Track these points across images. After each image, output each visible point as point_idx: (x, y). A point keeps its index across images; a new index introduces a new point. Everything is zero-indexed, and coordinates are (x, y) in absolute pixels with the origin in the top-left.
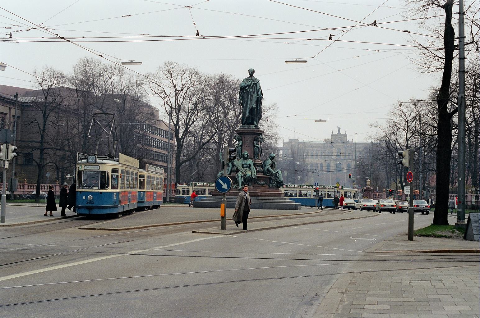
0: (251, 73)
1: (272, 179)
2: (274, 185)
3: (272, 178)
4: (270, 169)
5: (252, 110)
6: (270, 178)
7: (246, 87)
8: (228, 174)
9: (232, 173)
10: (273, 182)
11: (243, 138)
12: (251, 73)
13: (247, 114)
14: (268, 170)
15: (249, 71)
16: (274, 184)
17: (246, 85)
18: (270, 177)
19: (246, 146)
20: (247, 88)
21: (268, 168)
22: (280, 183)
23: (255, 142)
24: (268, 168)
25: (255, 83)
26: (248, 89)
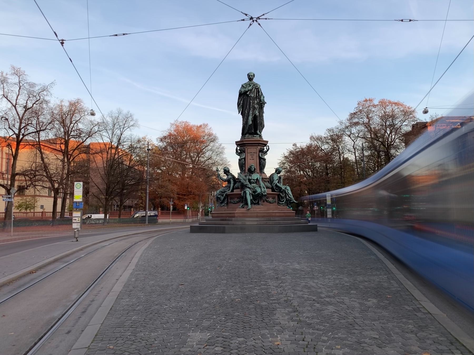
0: (251, 77)
1: (282, 197)
3: (281, 194)
4: (278, 184)
5: (255, 118)
6: (279, 195)
7: (247, 92)
8: (230, 191)
9: (235, 190)
11: (246, 149)
12: (251, 77)
13: (250, 122)
14: (276, 185)
15: (248, 75)
16: (283, 201)
18: (279, 194)
20: (248, 93)
22: (291, 200)
23: (260, 154)
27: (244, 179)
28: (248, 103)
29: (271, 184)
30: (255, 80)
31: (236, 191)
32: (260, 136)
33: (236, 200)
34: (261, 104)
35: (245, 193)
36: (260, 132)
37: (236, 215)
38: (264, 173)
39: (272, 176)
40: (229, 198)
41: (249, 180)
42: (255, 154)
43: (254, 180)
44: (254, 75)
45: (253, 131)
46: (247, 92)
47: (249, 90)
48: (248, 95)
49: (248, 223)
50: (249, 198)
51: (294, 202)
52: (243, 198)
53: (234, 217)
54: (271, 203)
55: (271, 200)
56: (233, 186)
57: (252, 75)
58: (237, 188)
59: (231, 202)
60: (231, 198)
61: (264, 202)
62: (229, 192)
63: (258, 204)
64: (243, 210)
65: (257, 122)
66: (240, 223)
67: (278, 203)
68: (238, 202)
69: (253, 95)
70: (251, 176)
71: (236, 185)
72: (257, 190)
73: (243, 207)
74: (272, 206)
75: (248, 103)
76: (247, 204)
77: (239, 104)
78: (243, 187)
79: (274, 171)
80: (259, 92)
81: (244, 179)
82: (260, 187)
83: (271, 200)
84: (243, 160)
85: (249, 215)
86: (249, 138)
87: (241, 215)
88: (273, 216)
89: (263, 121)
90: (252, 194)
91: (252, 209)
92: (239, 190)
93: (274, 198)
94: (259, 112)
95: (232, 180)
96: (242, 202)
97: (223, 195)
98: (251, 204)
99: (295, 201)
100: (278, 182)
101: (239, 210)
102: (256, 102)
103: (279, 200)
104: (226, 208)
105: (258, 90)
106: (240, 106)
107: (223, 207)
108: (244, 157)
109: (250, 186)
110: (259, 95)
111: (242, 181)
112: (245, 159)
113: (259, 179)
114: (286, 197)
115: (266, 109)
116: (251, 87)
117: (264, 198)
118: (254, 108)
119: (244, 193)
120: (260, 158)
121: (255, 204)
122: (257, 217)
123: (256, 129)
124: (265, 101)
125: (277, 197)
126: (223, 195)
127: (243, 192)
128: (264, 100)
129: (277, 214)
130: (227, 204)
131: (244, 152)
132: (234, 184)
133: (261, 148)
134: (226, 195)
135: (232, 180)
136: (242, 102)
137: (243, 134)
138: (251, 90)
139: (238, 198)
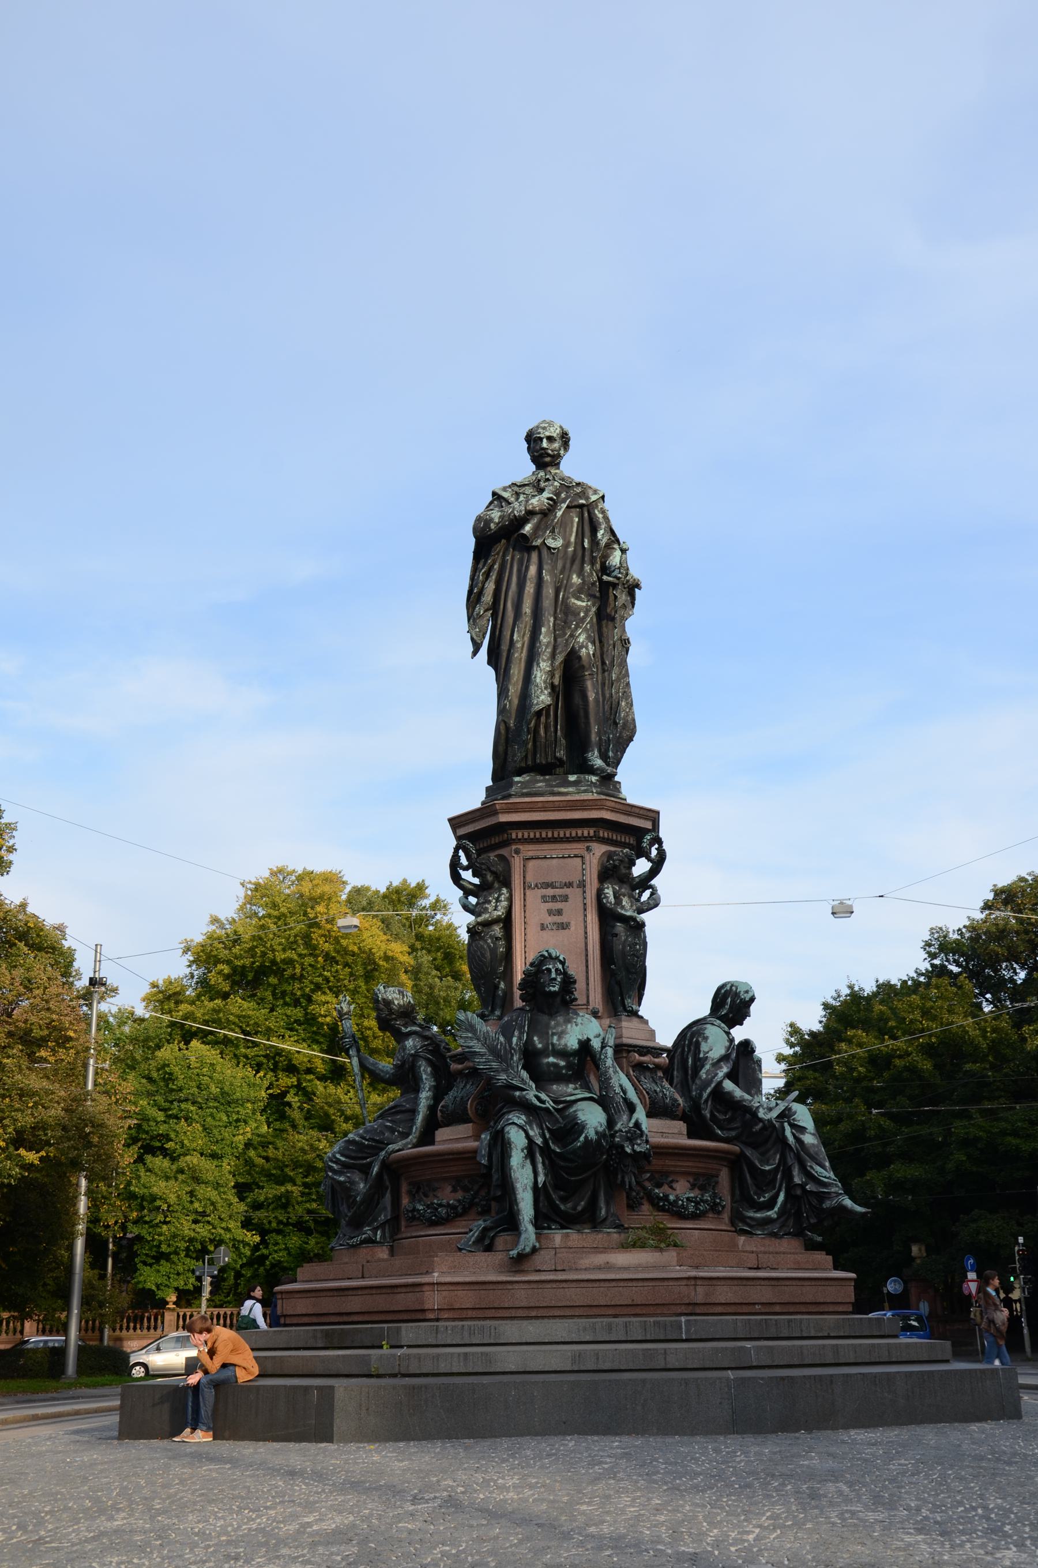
1: (753, 1170)
2: (772, 1214)
4: (729, 1085)
5: (571, 671)
7: (522, 521)
8: (412, 1138)
10: (761, 1192)
11: (517, 863)
12: (544, 451)
13: (542, 698)
14: (718, 1093)
16: (770, 1204)
17: (518, 508)
19: (543, 927)
20: (528, 528)
21: (720, 1083)
22: (822, 1197)
24: (720, 1083)
25: (581, 506)
26: (536, 529)
27: (493, 1051)
28: (530, 589)
29: (684, 1088)
30: (572, 466)
31: (451, 1138)
32: (608, 780)
33: (448, 1196)
34: (613, 595)
35: (501, 1145)
36: (604, 757)
37: (434, 1300)
38: (635, 1014)
39: (691, 1036)
40: (404, 1188)
41: (531, 1058)
42: (574, 893)
43: (563, 1053)
44: (565, 439)
45: (561, 754)
46: (522, 521)
47: (530, 513)
48: (525, 545)
49: (510, 1359)
50: (523, 1176)
51: (843, 1208)
52: (488, 1176)
53: (417, 1315)
54: (681, 1216)
55: (681, 1191)
56: (432, 1109)
57: (554, 432)
58: (456, 1117)
59: (415, 1217)
60: (418, 1190)
61: (633, 1206)
62: (403, 1148)
63: (588, 1219)
64: (483, 1267)
65: (585, 697)
66: (451, 1359)
67: (737, 1218)
68: (455, 1214)
69: (556, 543)
70: (544, 1035)
71: (448, 1100)
72: (582, 1117)
73: (486, 1243)
74: (691, 1233)
75: (530, 589)
76: (511, 1223)
77: (473, 598)
78: (494, 1103)
79: (703, 1009)
80: (594, 530)
81: (493, 1051)
82: (604, 1102)
83: (681, 1191)
84: (497, 930)
85: (521, 1297)
86: (540, 798)
87: (466, 1299)
88: (692, 1309)
89: (627, 695)
90: (545, 1150)
91: (543, 1260)
92: (464, 1130)
93: (704, 1182)
94: (600, 639)
95: (425, 1072)
96: (485, 1212)
97: (365, 1170)
98: (541, 1221)
99: (848, 1202)
100: (732, 1076)
101: (453, 1267)
102: (575, 579)
103: (744, 1198)
104: (383, 1253)
105: (587, 512)
106: (480, 609)
107: (364, 1252)
108: (500, 912)
109: (531, 1094)
110: (594, 542)
111: (484, 1062)
112: (507, 921)
113: (596, 1044)
114: (788, 1176)
115: (636, 625)
116: (546, 494)
117: (630, 1179)
118: (566, 615)
119: (492, 1145)
120: (607, 916)
121: (567, 1221)
122: (590, 1310)
123: (578, 744)
124: (636, 571)
125: (724, 1176)
126: (365, 1170)
127: (486, 1137)
128: (623, 567)
129: (724, 1294)
130: (393, 1226)
131: (507, 883)
132: (438, 1094)
133: (610, 856)
134: (385, 1165)
135: (425, 1072)
136: (490, 586)
137: (503, 769)
138: (546, 513)
139: (457, 1184)
